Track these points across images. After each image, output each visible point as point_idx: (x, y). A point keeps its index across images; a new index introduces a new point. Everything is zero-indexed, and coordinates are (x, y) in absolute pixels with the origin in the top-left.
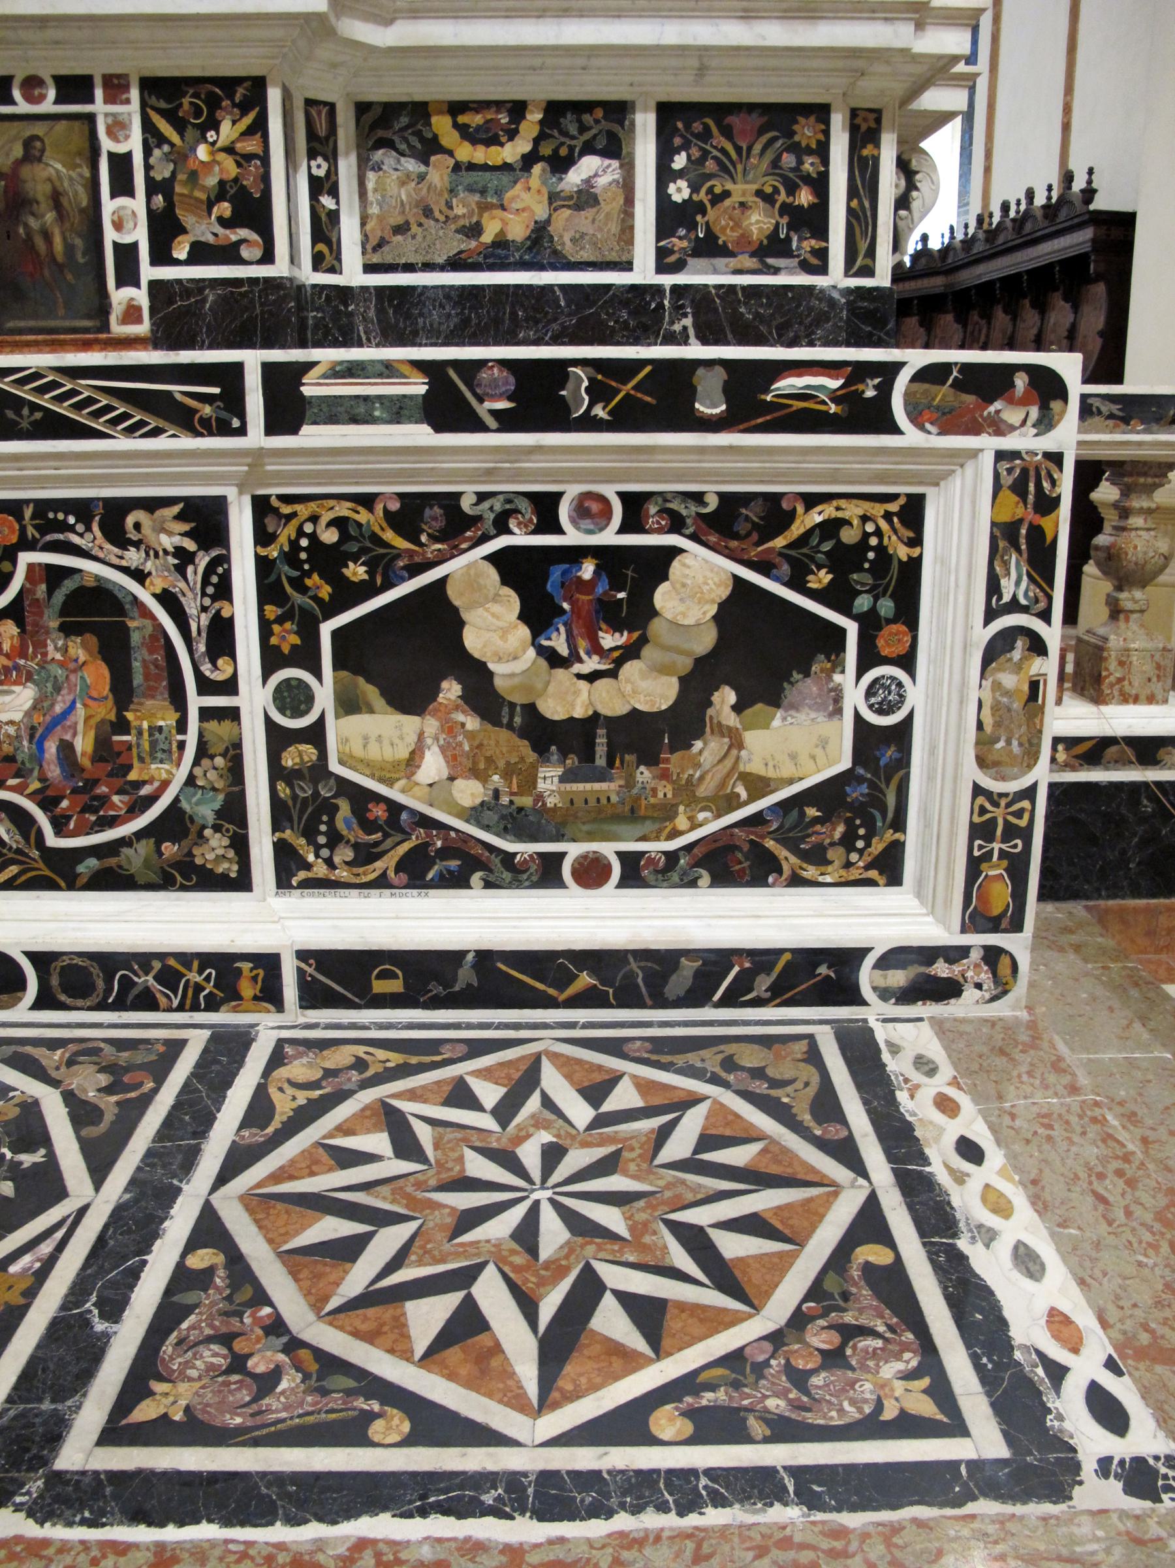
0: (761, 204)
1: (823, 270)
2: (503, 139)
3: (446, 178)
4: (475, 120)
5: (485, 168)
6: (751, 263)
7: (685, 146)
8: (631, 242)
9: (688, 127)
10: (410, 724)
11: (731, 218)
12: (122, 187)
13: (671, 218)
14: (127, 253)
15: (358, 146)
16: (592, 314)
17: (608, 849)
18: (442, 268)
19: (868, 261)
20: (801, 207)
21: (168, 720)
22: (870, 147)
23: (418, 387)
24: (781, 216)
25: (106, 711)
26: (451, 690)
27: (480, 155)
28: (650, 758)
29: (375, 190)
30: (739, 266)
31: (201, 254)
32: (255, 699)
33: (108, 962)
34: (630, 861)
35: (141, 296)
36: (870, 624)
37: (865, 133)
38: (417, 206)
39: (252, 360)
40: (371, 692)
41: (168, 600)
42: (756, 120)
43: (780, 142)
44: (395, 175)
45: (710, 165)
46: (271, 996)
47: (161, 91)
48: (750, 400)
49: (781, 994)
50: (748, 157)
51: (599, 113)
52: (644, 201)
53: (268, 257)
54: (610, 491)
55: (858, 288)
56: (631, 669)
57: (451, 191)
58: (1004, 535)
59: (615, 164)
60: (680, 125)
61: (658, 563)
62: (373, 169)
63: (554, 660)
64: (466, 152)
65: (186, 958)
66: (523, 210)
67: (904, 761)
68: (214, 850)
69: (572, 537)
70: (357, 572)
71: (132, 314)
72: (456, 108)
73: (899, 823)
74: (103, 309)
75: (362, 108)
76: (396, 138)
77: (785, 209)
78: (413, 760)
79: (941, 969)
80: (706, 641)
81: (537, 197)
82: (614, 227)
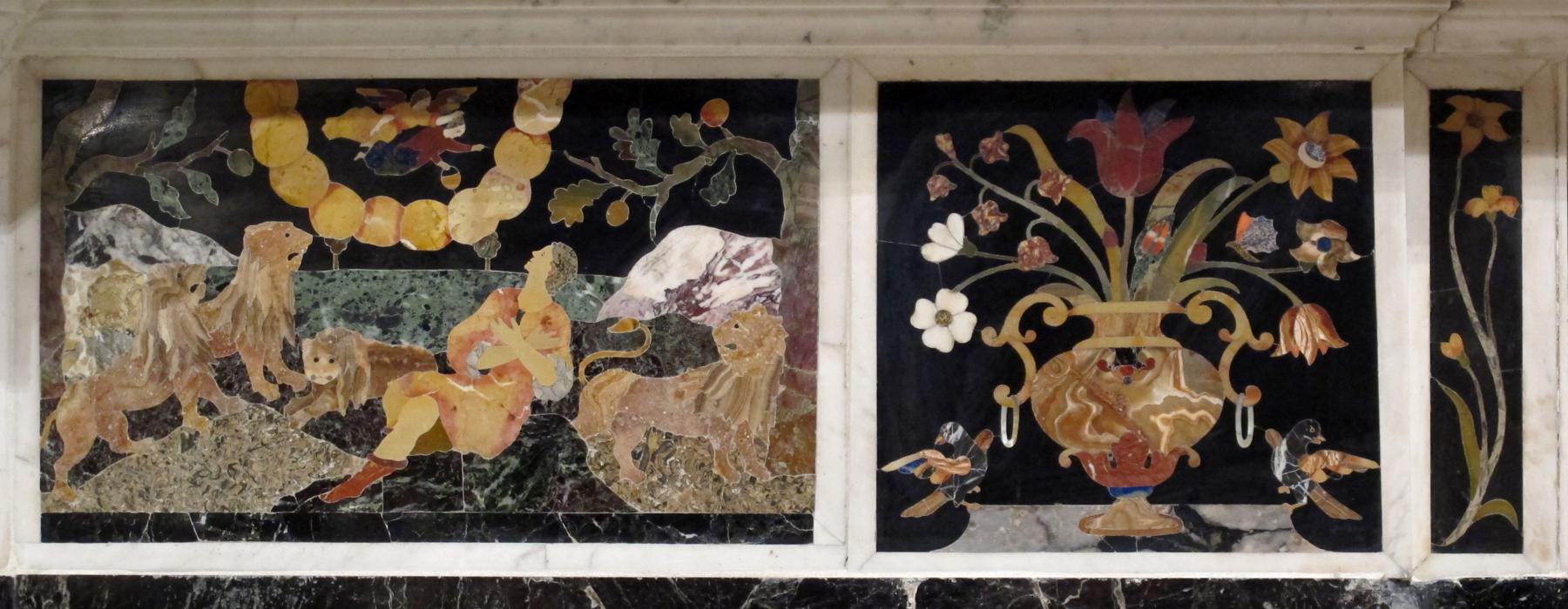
0: (1181, 354)
1: (1365, 535)
2: (450, 182)
3: (285, 284)
4: (371, 129)
5: (398, 257)
6: (1159, 518)
7: (961, 200)
8: (805, 460)
9: (966, 148)
11: (1093, 395)
13: (917, 393)
15: (46, 197)
18: (265, 530)
19: (1502, 507)
20: (1294, 362)
22: (1491, 192)
24: (1239, 387)
27: (383, 222)
29: (88, 314)
30: (1119, 528)
38: (201, 358)
42: (1162, 129)
43: (1227, 189)
44: (145, 273)
45: (1032, 252)
50: (1139, 226)
51: (718, 112)
52: (843, 347)
55: (1472, 585)
57: (300, 319)
59: (762, 247)
60: (944, 143)
62: (83, 258)
64: (343, 215)
66: (501, 372)
72: (320, 100)
76: (153, 179)
77: (1249, 368)
81: (546, 340)
82: (758, 421)
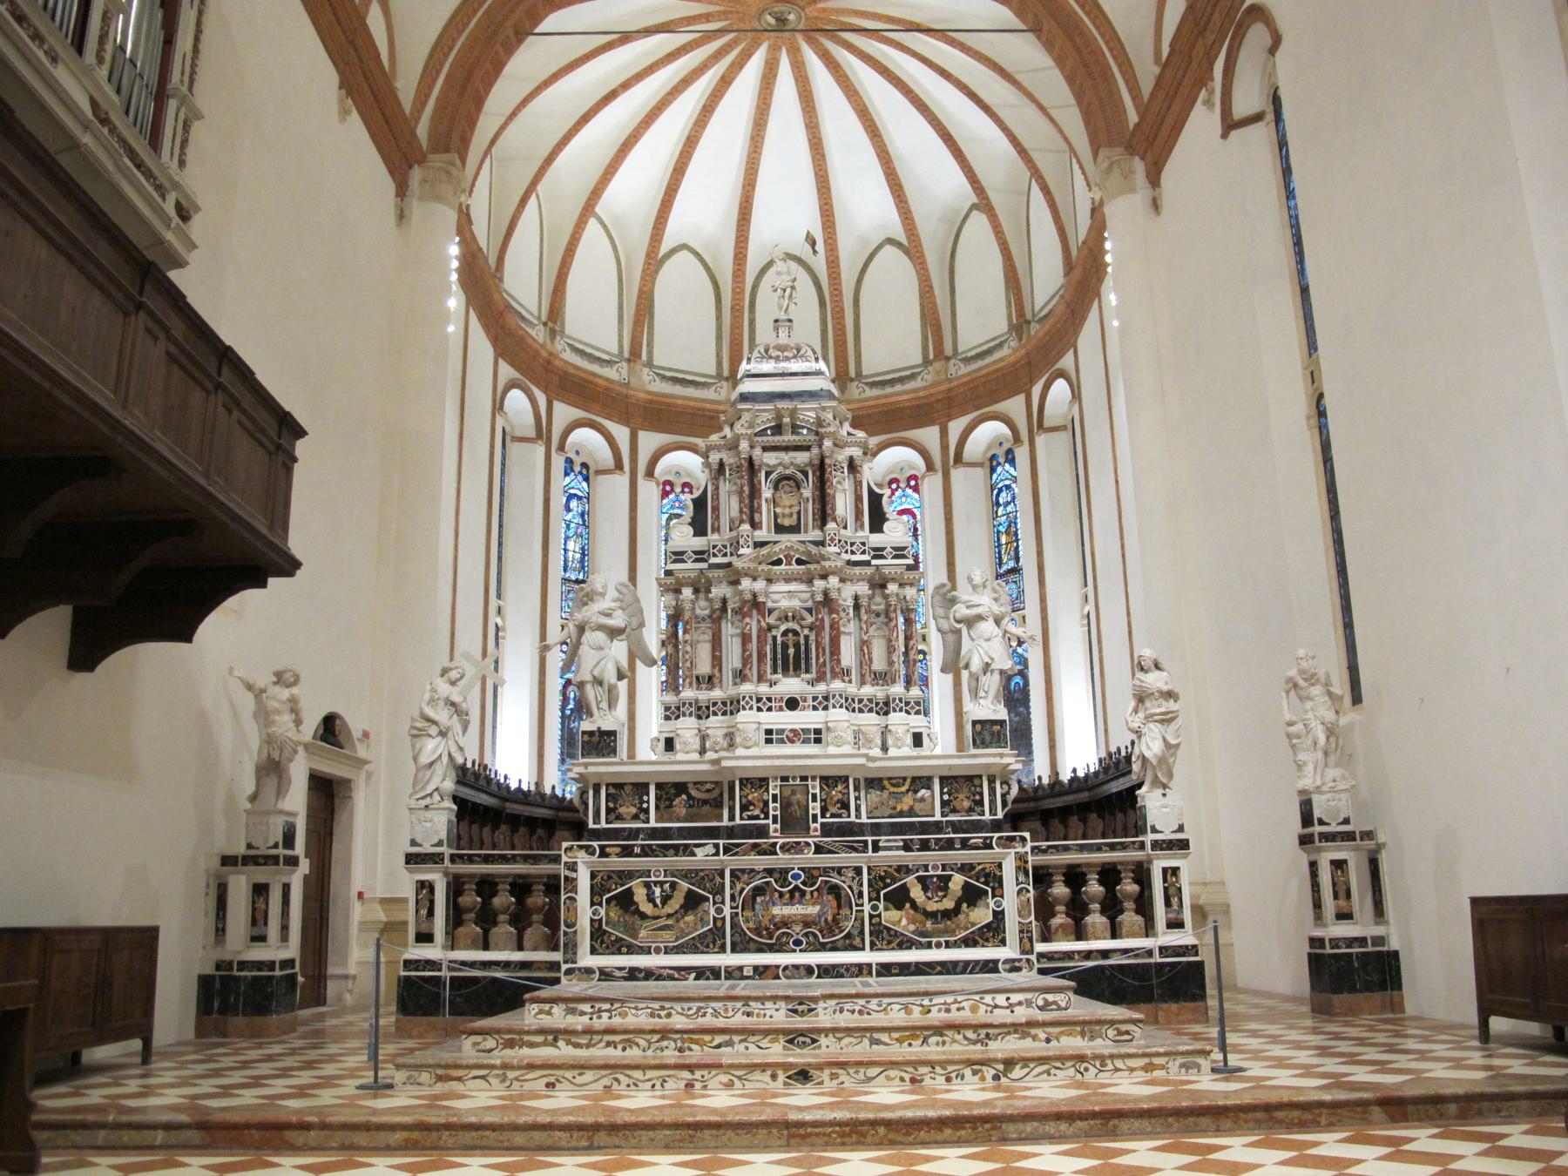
12: (814, 800)
13: (944, 804)
14: (815, 816)
31: (833, 816)
32: (867, 908)
33: (834, 966)
36: (993, 889)
37: (992, 780)
39: (870, 839)
46: (870, 974)
47: (825, 780)
48: (965, 844)
49: (982, 971)
58: (1018, 868)
64: (892, 789)
68: (857, 941)
69: (931, 873)
80: (960, 893)
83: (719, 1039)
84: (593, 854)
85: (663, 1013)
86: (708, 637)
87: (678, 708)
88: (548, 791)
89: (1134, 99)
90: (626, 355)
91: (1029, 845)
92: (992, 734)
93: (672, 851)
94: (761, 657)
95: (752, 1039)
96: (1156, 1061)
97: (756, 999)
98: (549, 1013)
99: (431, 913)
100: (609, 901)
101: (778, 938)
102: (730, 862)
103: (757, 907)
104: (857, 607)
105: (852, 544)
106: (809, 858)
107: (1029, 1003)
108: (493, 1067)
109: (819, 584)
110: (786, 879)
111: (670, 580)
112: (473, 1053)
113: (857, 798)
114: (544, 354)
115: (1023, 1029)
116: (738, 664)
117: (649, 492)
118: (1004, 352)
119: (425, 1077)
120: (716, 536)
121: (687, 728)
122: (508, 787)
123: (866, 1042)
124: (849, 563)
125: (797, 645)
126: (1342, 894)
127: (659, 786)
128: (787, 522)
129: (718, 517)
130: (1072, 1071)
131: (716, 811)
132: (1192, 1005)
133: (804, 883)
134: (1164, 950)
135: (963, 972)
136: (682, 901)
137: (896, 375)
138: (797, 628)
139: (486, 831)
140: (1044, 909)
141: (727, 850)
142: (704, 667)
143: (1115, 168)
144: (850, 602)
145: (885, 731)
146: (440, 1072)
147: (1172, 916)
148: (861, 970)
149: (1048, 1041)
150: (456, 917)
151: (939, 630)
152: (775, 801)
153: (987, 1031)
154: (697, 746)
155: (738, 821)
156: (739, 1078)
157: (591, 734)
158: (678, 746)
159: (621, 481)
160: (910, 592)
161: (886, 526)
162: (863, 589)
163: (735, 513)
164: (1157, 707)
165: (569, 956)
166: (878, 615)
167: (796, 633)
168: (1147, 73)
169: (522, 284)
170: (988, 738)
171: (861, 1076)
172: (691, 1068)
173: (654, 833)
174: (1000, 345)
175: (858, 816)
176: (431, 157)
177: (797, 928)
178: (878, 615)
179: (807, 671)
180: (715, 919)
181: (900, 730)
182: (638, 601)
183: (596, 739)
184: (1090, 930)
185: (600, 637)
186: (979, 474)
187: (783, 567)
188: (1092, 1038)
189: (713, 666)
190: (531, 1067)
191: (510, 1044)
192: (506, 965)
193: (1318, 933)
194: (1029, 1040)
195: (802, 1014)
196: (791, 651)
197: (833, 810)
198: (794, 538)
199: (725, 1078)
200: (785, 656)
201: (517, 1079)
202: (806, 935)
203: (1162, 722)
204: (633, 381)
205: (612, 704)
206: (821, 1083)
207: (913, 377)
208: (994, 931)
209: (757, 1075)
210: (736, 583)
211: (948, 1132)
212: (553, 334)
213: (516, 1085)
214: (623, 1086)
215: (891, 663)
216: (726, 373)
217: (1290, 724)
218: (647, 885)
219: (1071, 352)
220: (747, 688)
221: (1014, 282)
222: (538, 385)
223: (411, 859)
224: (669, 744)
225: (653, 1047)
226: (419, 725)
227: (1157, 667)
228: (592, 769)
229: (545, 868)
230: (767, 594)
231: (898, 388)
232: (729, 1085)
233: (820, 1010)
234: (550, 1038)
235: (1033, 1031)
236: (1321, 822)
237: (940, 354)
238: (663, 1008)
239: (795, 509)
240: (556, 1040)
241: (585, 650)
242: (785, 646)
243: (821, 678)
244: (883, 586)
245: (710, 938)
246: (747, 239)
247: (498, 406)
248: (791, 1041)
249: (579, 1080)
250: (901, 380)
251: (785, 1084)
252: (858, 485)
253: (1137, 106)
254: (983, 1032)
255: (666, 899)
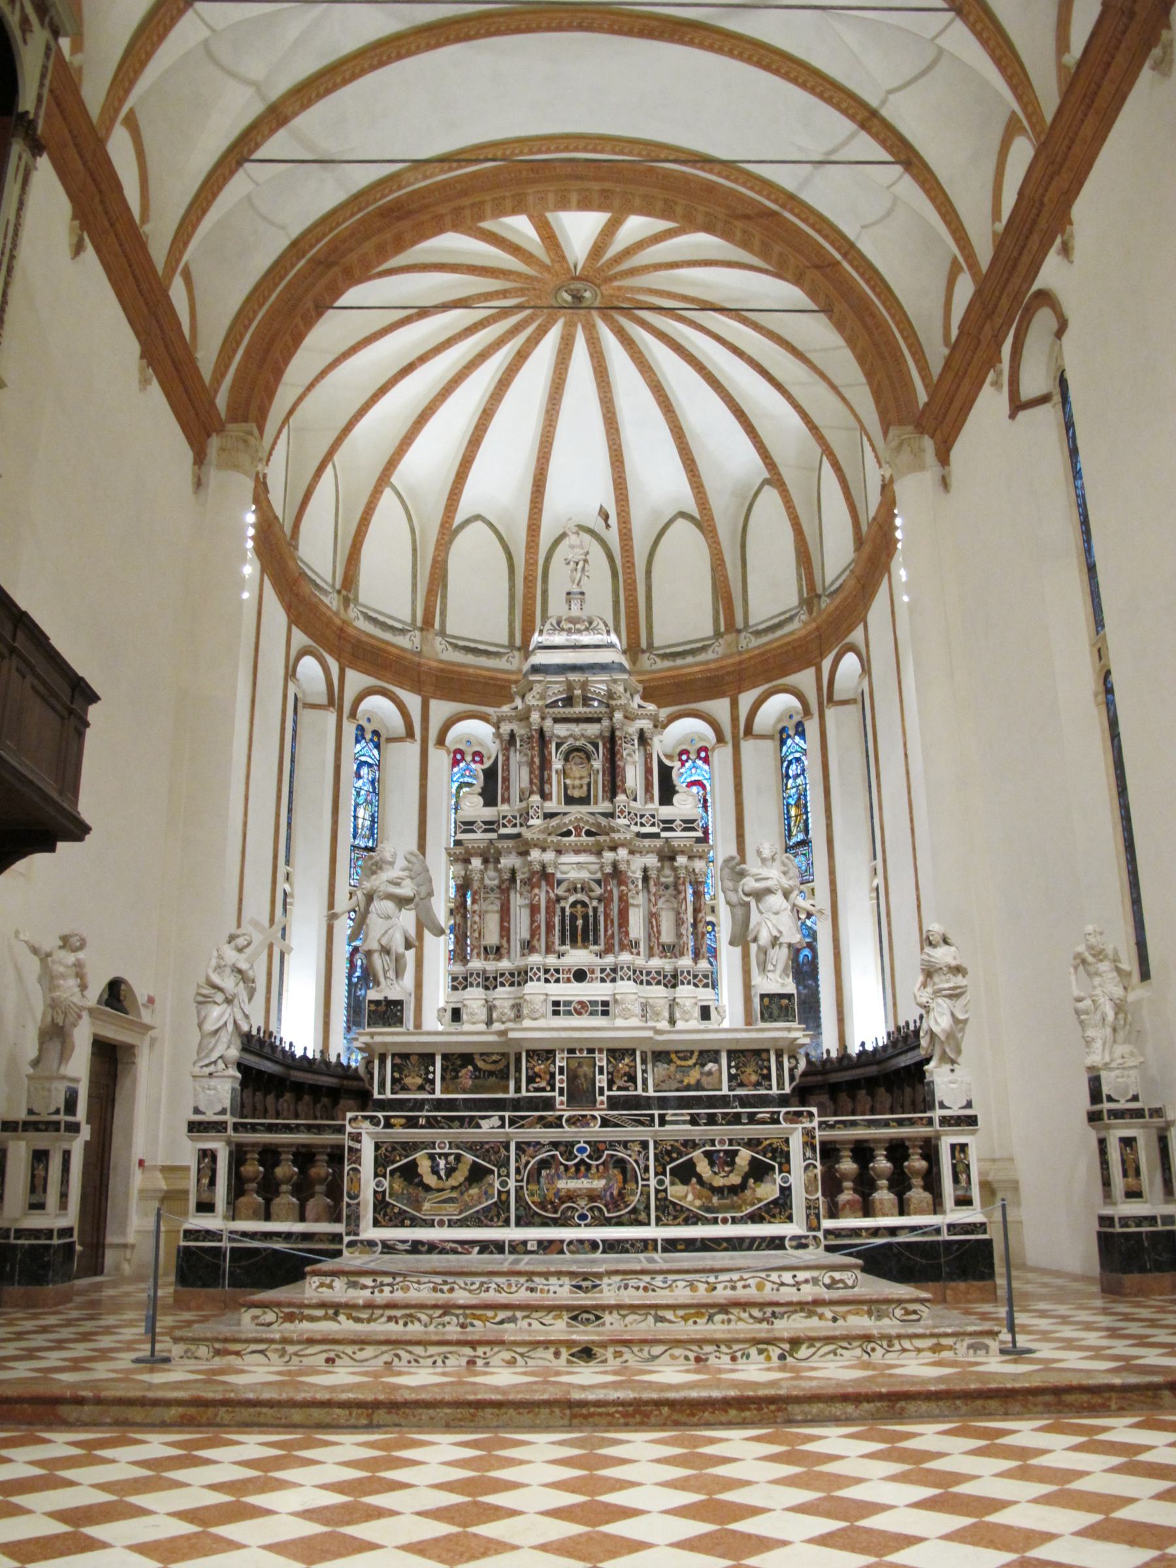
4: (681, 1055)
10: (685, 1188)
12: (601, 1073)
13: (731, 1078)
14: (601, 1089)
16: (712, 1102)
17: (728, 1215)
21: (634, 1187)
23: (688, 1118)
25: (621, 1185)
26: (694, 1180)
27: (683, 1063)
28: (736, 1194)
31: (619, 1089)
32: (653, 1183)
33: (619, 1241)
34: (733, 1218)
35: (604, 1098)
36: (780, 1164)
37: (779, 1055)
39: (656, 1113)
40: (677, 1181)
41: (636, 1161)
46: (656, 1249)
47: (612, 1052)
48: (752, 1119)
49: (768, 1248)
53: (636, 1089)
54: (725, 1138)
56: (731, 1175)
58: (805, 1144)
61: (736, 1153)
63: (715, 1173)
64: (679, 1063)
65: (637, 1240)
67: (790, 1195)
68: (643, 1216)
69: (718, 1147)
70: (674, 1155)
71: (602, 1103)
72: (677, 1052)
73: (791, 1208)
74: (595, 1101)
75: (653, 1052)
78: (686, 1196)
79: (803, 1241)
80: (746, 1169)
83: (502, 1315)
84: (377, 1124)
85: (445, 1288)
86: (496, 907)
87: (465, 979)
88: (333, 1059)
89: (923, 379)
90: (419, 624)
91: (817, 1120)
92: (781, 1008)
93: (457, 1123)
94: (550, 928)
95: (535, 1315)
96: (945, 1341)
97: (540, 1274)
98: (330, 1286)
99: (212, 1182)
100: (392, 1172)
101: (563, 1213)
102: (516, 1135)
103: (542, 1180)
104: (646, 879)
105: (642, 816)
106: (595, 1131)
107: (815, 1281)
108: (272, 1341)
109: (608, 856)
110: (571, 1153)
111: (459, 850)
112: (253, 1327)
113: (644, 1071)
114: (338, 622)
115: (809, 1307)
116: (526, 935)
117: (439, 759)
118: (795, 625)
119: (203, 1351)
120: (505, 807)
121: (474, 998)
122: (293, 1055)
123: (651, 1319)
124: (639, 835)
125: (585, 917)
126: (1131, 1172)
127: (445, 1057)
128: (576, 794)
129: (508, 788)
130: (858, 1352)
131: (503, 1083)
132: (981, 1284)
133: (589, 1157)
134: (952, 1228)
135: (750, 1248)
136: (466, 1173)
137: (688, 647)
138: (586, 900)
139: (270, 1098)
140: (832, 1184)
141: (513, 1122)
142: (492, 938)
143: (906, 448)
144: (639, 875)
145: (673, 1004)
146: (218, 1346)
147: (960, 1193)
148: (647, 1245)
149: (835, 1320)
150: (238, 1188)
151: (728, 903)
152: (561, 1073)
153: (772, 1309)
154: (484, 1017)
155: (524, 1093)
156: (522, 1355)
157: (377, 1003)
158: (464, 1017)
159: (412, 749)
160: (699, 865)
161: (676, 799)
162: (652, 861)
163: (525, 783)
164: (946, 982)
165: (352, 1227)
166: (667, 887)
167: (584, 905)
168: (937, 354)
169: (317, 552)
170: (776, 1012)
171: (645, 1354)
172: (473, 1344)
173: (439, 1105)
174: (791, 619)
175: (645, 1089)
176: (229, 426)
177: (583, 1203)
178: (667, 887)
179: (596, 943)
180: (500, 1192)
181: (688, 1003)
182: (427, 871)
183: (382, 1008)
184: (878, 1206)
185: (389, 906)
186: (770, 746)
187: (572, 838)
188: (879, 1318)
189: (502, 937)
190: (311, 1341)
191: (290, 1318)
192: (288, 1236)
193: (1107, 1211)
194: (816, 1318)
195: (587, 1290)
196: (580, 922)
197: (620, 1083)
198: (584, 809)
199: (507, 1355)
200: (574, 927)
201: (296, 1354)
202: (591, 1209)
203: (950, 997)
204: (425, 649)
205: (399, 973)
206: (605, 1361)
207: (704, 649)
208: (781, 1207)
209: (540, 1353)
210: (524, 853)
211: (733, 1413)
212: (346, 602)
213: (295, 1359)
214: (404, 1362)
215: (679, 936)
216: (518, 643)
217: (1079, 1000)
218: (432, 1157)
219: (861, 626)
220: (535, 959)
221: (804, 557)
222: (330, 653)
223: (193, 1127)
224: (456, 1015)
225: (435, 1322)
226: (204, 992)
227: (946, 941)
228: (378, 1039)
229: (329, 1138)
230: (556, 867)
231: (690, 660)
232: (512, 1363)
233: (604, 1286)
234: (331, 1312)
235: (820, 1310)
236: (1110, 1099)
237: (731, 626)
238: (445, 1283)
239: (585, 781)
240: (336, 1314)
241: (373, 919)
242: (573, 918)
243: (609, 950)
244: (673, 859)
245: (494, 1212)
246: (541, 510)
247: (291, 673)
248: (574, 1318)
249: (360, 1355)
250: (692, 652)
251: (569, 1361)
252: (648, 757)
253: (926, 386)
254: (769, 1310)
255: (450, 1171)
